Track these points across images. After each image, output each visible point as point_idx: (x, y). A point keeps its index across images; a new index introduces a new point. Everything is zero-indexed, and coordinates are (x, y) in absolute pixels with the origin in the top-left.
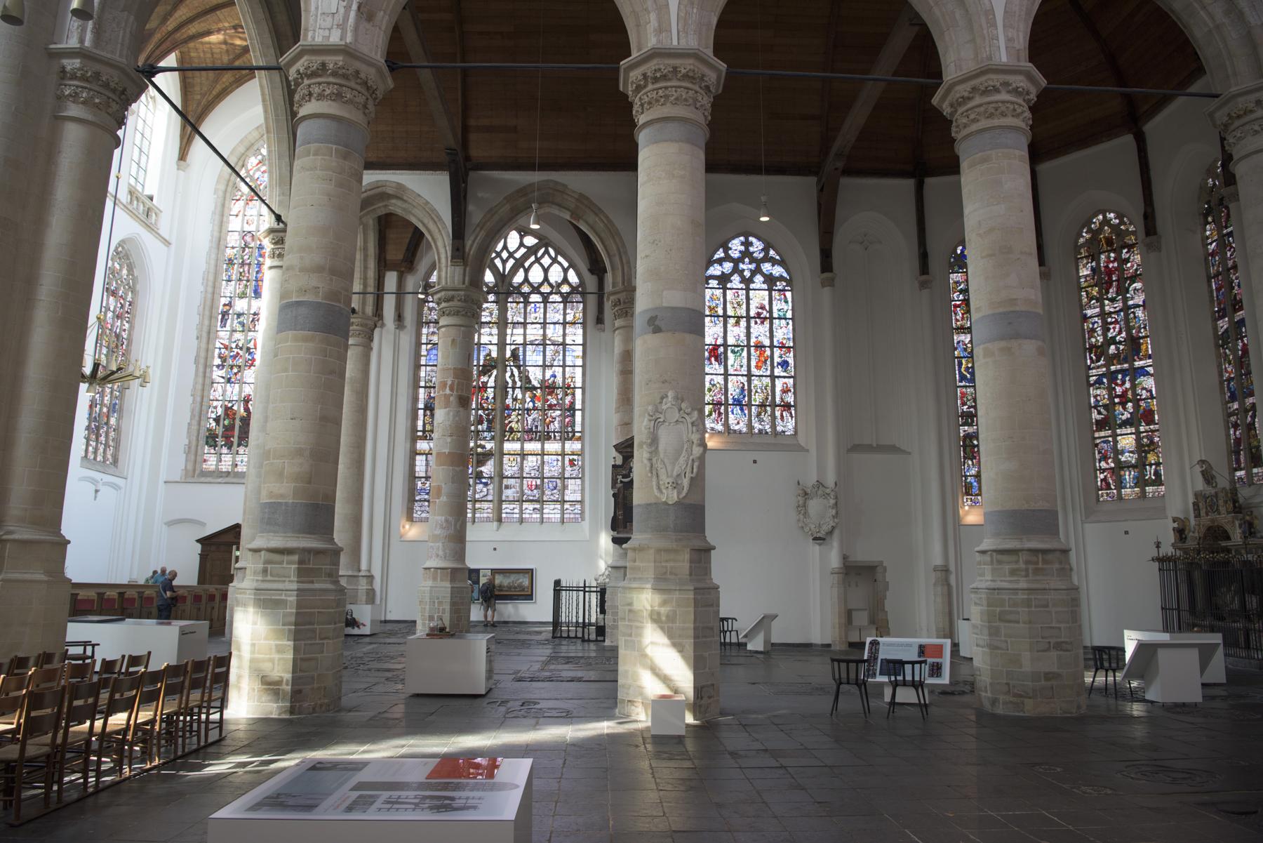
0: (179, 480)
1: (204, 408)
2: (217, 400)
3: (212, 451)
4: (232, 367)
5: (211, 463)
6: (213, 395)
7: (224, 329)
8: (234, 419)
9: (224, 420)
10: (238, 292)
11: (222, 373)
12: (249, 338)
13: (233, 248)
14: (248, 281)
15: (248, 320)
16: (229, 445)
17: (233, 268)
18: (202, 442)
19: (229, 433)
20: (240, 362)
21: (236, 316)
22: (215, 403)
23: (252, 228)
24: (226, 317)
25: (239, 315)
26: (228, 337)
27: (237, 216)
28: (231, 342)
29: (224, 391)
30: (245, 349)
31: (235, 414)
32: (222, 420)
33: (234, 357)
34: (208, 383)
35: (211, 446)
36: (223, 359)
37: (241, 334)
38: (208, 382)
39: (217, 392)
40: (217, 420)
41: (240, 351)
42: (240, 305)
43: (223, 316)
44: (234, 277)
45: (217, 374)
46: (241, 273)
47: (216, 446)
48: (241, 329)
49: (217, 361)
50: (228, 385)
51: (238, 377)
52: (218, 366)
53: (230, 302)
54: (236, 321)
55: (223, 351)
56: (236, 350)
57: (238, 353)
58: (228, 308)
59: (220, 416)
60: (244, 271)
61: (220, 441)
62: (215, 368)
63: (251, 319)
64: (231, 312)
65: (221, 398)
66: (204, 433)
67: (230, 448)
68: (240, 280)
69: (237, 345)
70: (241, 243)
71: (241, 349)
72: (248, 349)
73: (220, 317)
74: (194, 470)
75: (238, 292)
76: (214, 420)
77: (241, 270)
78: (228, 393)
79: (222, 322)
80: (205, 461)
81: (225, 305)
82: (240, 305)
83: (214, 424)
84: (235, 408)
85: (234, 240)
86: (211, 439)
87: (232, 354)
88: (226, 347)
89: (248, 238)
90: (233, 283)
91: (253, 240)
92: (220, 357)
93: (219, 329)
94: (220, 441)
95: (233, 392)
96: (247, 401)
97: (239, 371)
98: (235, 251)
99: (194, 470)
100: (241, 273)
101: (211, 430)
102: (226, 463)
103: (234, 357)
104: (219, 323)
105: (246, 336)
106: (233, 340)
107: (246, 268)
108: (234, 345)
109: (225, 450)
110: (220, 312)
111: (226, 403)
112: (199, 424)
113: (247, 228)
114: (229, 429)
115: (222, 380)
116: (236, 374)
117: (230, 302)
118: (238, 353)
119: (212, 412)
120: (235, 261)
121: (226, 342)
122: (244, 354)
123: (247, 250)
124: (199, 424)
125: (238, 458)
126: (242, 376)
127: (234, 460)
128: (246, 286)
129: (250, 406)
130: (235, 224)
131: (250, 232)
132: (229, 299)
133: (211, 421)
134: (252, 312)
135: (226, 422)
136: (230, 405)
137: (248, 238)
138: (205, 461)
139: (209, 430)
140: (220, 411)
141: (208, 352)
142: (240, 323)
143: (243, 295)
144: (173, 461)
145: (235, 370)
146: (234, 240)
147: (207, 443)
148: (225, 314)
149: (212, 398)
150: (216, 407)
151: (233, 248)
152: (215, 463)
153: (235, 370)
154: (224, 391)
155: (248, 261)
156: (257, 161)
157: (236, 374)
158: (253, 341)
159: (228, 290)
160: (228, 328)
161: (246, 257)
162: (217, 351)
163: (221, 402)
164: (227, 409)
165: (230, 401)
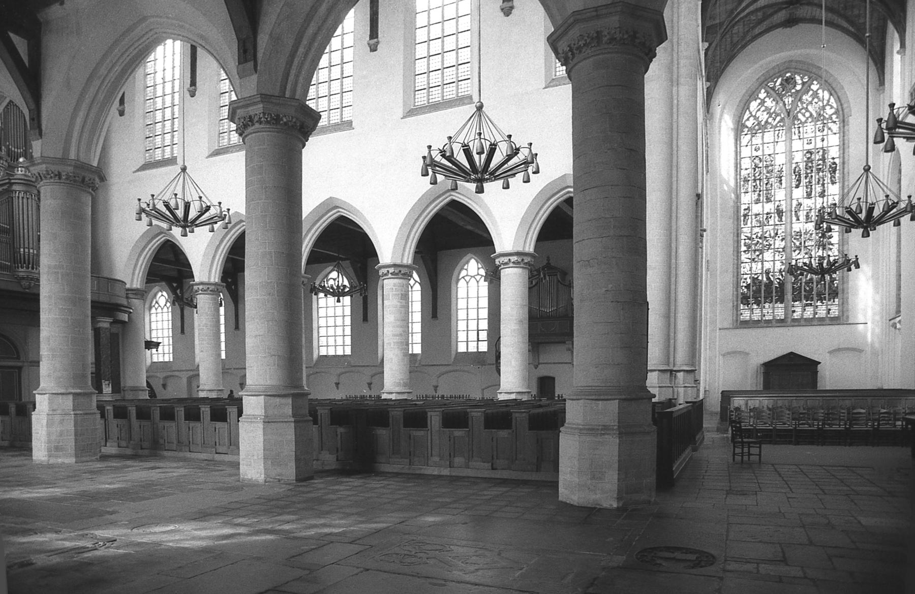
0: (728, 327)
1: (739, 280)
2: (746, 274)
3: (746, 308)
4: (755, 251)
5: (746, 315)
6: (742, 271)
7: (746, 226)
8: (760, 286)
9: (753, 286)
10: (753, 199)
11: (747, 256)
12: (765, 231)
13: (746, 169)
14: (760, 191)
15: (763, 218)
16: (758, 303)
17: (748, 184)
18: (739, 302)
19: (758, 295)
20: (759, 247)
21: (753, 217)
22: (745, 276)
23: (759, 153)
24: (747, 218)
25: (756, 215)
26: (750, 231)
27: (747, 146)
28: (751, 235)
29: (751, 268)
30: (763, 239)
31: (760, 282)
32: (751, 287)
33: (756, 245)
34: (738, 263)
35: (745, 304)
36: (749, 246)
37: (759, 228)
38: (739, 263)
39: (745, 269)
40: (748, 287)
41: (759, 240)
42: (756, 209)
43: (745, 218)
44: (750, 190)
45: (744, 257)
46: (754, 186)
47: (749, 304)
48: (758, 225)
49: (743, 248)
50: (753, 264)
51: (760, 257)
52: (745, 251)
53: (749, 207)
54: (754, 220)
55: (747, 241)
56: (756, 240)
57: (758, 241)
58: (747, 211)
59: (750, 284)
60: (756, 185)
61: (751, 300)
62: (742, 253)
63: (765, 217)
64: (750, 214)
65: (749, 272)
66: (740, 296)
67: (758, 305)
68: (754, 191)
69: (757, 237)
70: (752, 165)
71: (760, 238)
72: (766, 237)
73: (742, 218)
74: (737, 320)
75: (753, 199)
76: (745, 287)
77: (755, 184)
78: (754, 269)
79: (744, 221)
80: (742, 314)
81: (745, 210)
82: (756, 209)
83: (746, 290)
84: (760, 278)
85: (746, 163)
86: (745, 300)
87: (754, 242)
88: (749, 239)
89: (757, 161)
90: (750, 194)
91: (761, 161)
92: (745, 246)
93: (742, 226)
94: (751, 300)
95: (757, 268)
96: (768, 273)
97: (760, 254)
98: (748, 171)
99: (737, 320)
100: (754, 186)
101: (744, 294)
102: (756, 317)
103: (756, 245)
104: (742, 222)
105: (763, 229)
106: (754, 233)
107: (758, 182)
108: (754, 236)
109: (755, 306)
110: (742, 215)
111: (753, 275)
112: (737, 291)
113: (755, 154)
114: (758, 291)
115: (749, 261)
116: (758, 256)
117: (749, 207)
118: (758, 241)
119: (744, 282)
120: (749, 179)
121: (749, 235)
122: (763, 241)
123: (757, 169)
124: (737, 291)
125: (765, 311)
126: (763, 257)
127: (762, 313)
128: (759, 195)
129: (770, 276)
130: (746, 152)
131: (757, 157)
132: (747, 205)
133: (743, 288)
134: (765, 212)
135: (754, 288)
136: (756, 276)
137: (757, 161)
138: (742, 314)
139: (742, 294)
140: (749, 281)
141: (738, 242)
142: (757, 221)
143: (757, 201)
144: (724, 317)
145: (757, 253)
146: (746, 163)
147: (742, 303)
148: (745, 216)
149: (742, 273)
150: (746, 279)
151: (746, 169)
152: (749, 315)
153: (757, 253)
154: (751, 268)
155: (758, 177)
156: (758, 104)
157: (758, 256)
158: (768, 233)
159: (746, 199)
160: (749, 225)
161: (757, 175)
162: (743, 242)
163: (749, 275)
164: (754, 279)
165: (755, 274)
